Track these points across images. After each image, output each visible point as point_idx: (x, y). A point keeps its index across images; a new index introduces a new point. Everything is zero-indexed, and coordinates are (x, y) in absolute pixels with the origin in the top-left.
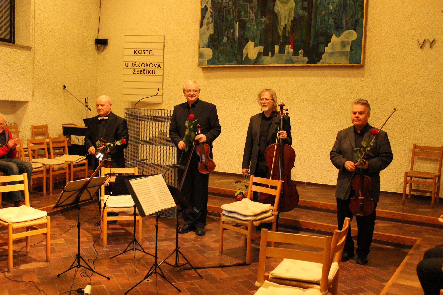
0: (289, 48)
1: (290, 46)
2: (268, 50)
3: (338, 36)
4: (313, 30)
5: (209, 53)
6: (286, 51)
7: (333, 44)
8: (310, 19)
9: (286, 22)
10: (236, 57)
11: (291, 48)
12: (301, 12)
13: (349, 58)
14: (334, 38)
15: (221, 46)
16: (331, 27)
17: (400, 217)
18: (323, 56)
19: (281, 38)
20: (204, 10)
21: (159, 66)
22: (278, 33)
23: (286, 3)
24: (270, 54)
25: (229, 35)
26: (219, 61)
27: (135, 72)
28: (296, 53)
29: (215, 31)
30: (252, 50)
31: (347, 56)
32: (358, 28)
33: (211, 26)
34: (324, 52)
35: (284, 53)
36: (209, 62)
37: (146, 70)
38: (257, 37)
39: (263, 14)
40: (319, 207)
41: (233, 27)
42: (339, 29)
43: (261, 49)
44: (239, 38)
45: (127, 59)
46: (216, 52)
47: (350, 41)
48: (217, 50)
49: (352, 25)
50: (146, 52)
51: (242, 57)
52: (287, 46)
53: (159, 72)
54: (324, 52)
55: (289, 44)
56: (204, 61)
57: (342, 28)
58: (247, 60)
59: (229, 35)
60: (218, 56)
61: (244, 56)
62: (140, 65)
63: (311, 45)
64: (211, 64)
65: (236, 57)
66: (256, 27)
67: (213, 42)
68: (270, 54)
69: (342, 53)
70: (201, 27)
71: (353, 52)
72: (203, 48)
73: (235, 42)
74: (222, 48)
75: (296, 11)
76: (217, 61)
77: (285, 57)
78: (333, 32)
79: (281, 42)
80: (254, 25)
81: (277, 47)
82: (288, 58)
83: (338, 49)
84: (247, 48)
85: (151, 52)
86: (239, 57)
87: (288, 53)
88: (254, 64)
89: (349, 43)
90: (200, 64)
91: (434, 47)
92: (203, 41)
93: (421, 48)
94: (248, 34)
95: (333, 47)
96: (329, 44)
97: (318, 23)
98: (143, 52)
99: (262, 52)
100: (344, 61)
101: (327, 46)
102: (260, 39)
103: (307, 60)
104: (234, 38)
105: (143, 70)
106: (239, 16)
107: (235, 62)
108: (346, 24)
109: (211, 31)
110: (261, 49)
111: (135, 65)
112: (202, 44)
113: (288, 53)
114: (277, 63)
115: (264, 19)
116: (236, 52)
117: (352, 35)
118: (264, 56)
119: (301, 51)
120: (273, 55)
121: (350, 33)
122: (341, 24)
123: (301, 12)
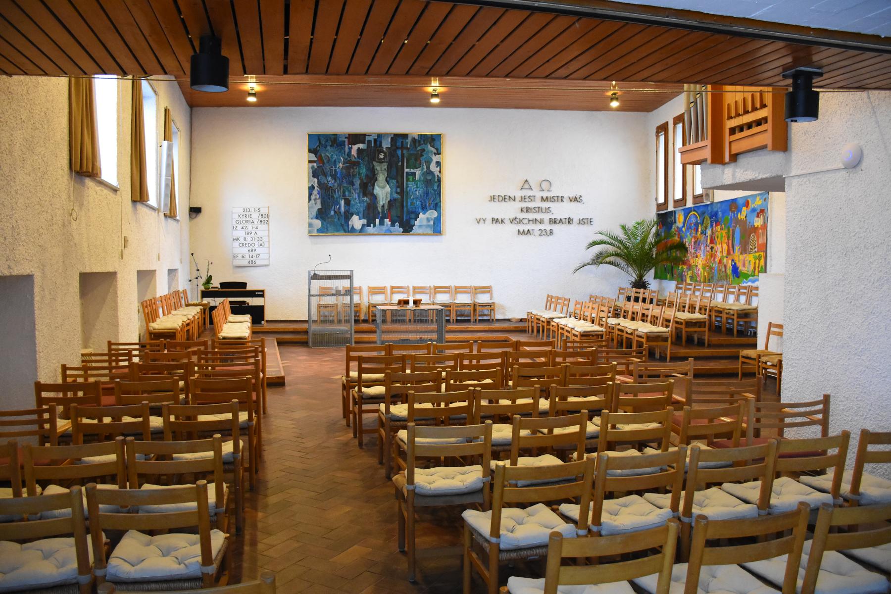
0: (387, 221)
2: (370, 222)
3: (424, 214)
4: (405, 209)
5: (318, 223)
8: (403, 201)
12: (395, 196)
14: (421, 215)
20: (311, 188)
23: (383, 188)
28: (393, 225)
30: (357, 222)
33: (319, 202)
36: (318, 231)
39: (365, 195)
41: (339, 204)
42: (424, 208)
43: (365, 221)
61: (350, 227)
67: (321, 214)
69: (428, 226)
75: (391, 194)
77: (384, 228)
81: (377, 221)
83: (425, 223)
86: (346, 228)
94: (352, 210)
95: (421, 221)
97: (409, 204)
100: (430, 231)
106: (344, 195)
109: (319, 206)
110: (365, 221)
115: (365, 199)
117: (435, 214)
120: (375, 226)
123: (395, 196)
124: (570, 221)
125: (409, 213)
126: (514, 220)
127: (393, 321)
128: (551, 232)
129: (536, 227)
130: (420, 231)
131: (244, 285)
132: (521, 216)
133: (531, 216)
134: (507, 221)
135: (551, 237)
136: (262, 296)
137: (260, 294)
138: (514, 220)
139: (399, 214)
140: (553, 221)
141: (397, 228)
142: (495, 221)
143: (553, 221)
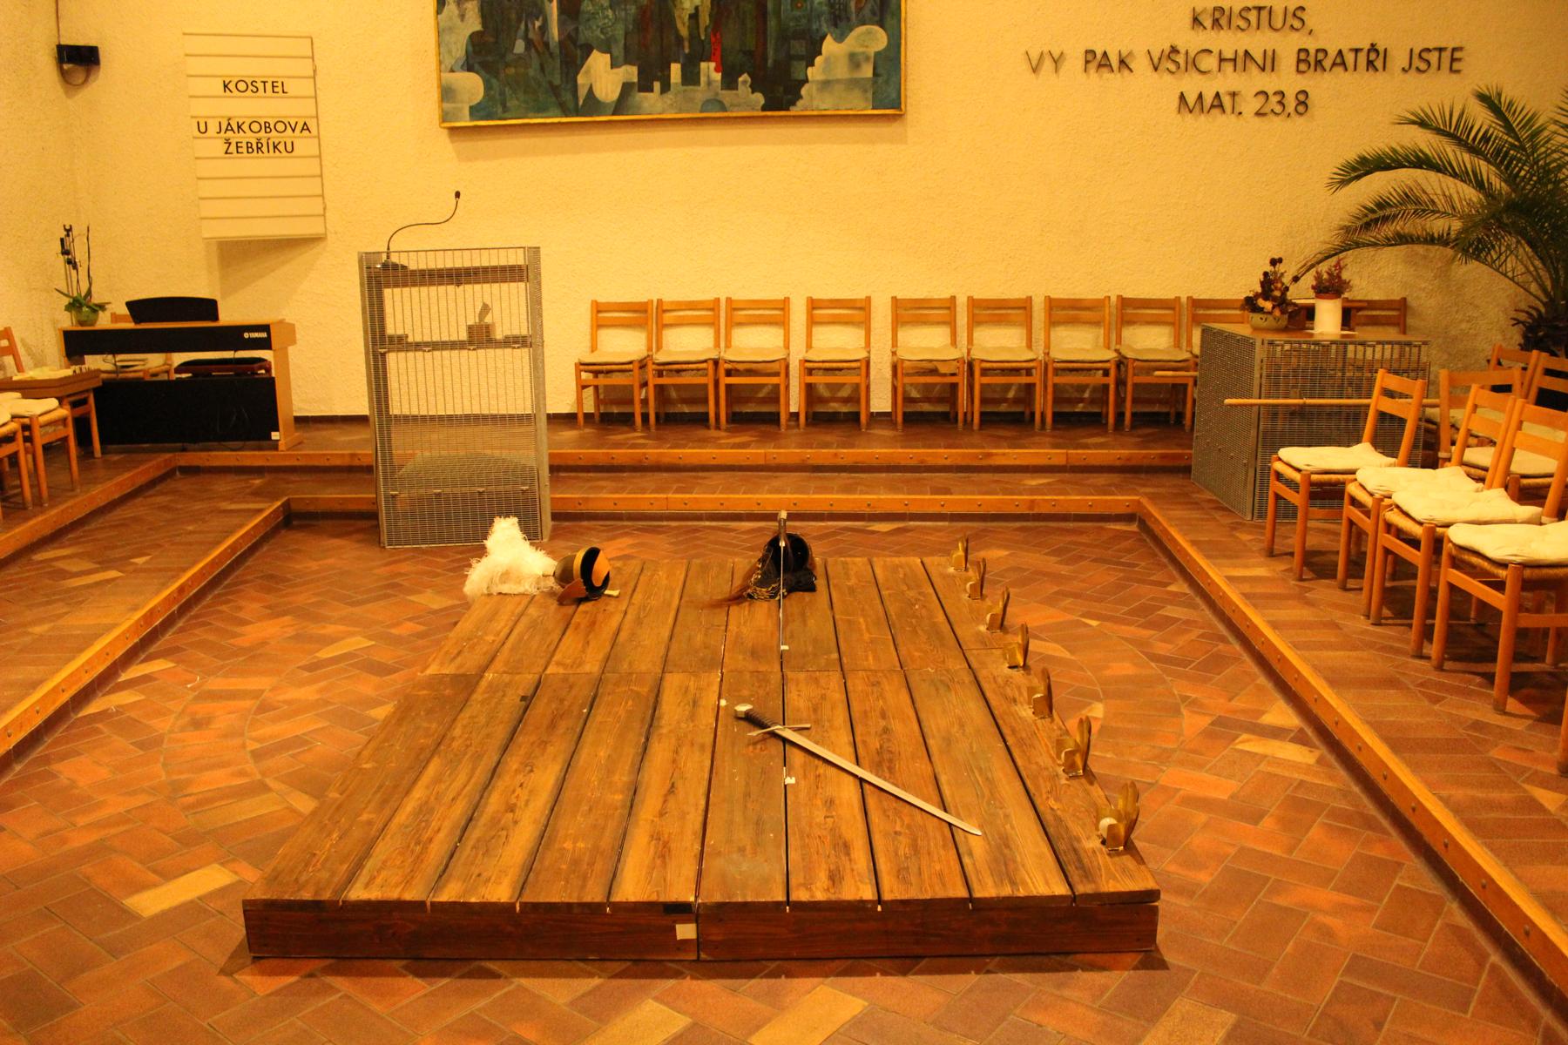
0: (709, 70)
1: (713, 65)
2: (651, 76)
3: (840, 39)
4: (772, 23)
5: (472, 86)
6: (703, 79)
7: (827, 60)
9: (697, 1)
10: (557, 95)
11: (717, 70)
13: (870, 95)
14: (829, 45)
15: (507, 65)
16: (819, 16)
17: (1061, 461)
18: (803, 91)
19: (686, 44)
21: (306, 127)
22: (677, 31)
24: (657, 86)
25: (531, 35)
26: (505, 109)
27: (232, 149)
28: (730, 82)
29: (484, 24)
30: (603, 76)
31: (865, 91)
32: (889, 21)
34: (806, 81)
35: (696, 82)
36: (475, 112)
37: (264, 141)
38: (616, 41)
40: (875, 463)
41: (540, 12)
42: (841, 22)
43: (631, 73)
44: (561, 42)
45: (202, 109)
46: (494, 81)
47: (872, 51)
48: (496, 75)
49: (874, 14)
50: (260, 86)
51: (576, 97)
52: (703, 65)
53: (304, 145)
54: (806, 81)
55: (708, 60)
56: (460, 110)
57: (849, 19)
58: (592, 105)
59: (531, 35)
60: (502, 93)
61: (582, 93)
62: (245, 127)
63: (770, 62)
64: (482, 119)
65: (557, 95)
66: (610, 13)
67: (482, 54)
68: (657, 86)
69: (853, 83)
70: (439, 11)
71: (880, 80)
72: (452, 71)
73: (551, 54)
74: (512, 71)
76: (500, 110)
77: (700, 93)
78: (825, 28)
79: (686, 56)
80: (603, 8)
81: (676, 70)
82: (709, 95)
83: (842, 71)
84: (588, 72)
85: (276, 87)
86: (567, 96)
87: (709, 83)
88: (614, 114)
89: (867, 59)
90: (445, 117)
91: (1062, 71)
92: (450, 52)
93: (1035, 70)
96: (818, 60)
98: (251, 86)
99: (635, 80)
101: (812, 65)
102: (626, 47)
103: (762, 101)
104: (547, 45)
105: (254, 142)
107: (558, 111)
108: (859, 10)
109: (474, 24)
110: (631, 73)
111: (229, 128)
112: (449, 62)
113: (709, 83)
114: (680, 111)
116: (557, 82)
117: (878, 39)
118: (640, 90)
119: (745, 77)
120: (666, 88)
121: (869, 33)
122: (846, 7)
124: (1374, 58)
125: (784, 37)
126: (1170, 59)
127: (739, 420)
128: (1303, 101)
129: (1249, 83)
130: (825, 104)
131: (208, 308)
132: (1191, 41)
133: (1229, 42)
134: (1140, 64)
135: (1300, 120)
136: (265, 344)
137: (262, 336)
138: (1170, 59)
139: (751, 43)
140: (1310, 61)
141: (747, 96)
142: (1097, 61)
143: (1310, 61)
